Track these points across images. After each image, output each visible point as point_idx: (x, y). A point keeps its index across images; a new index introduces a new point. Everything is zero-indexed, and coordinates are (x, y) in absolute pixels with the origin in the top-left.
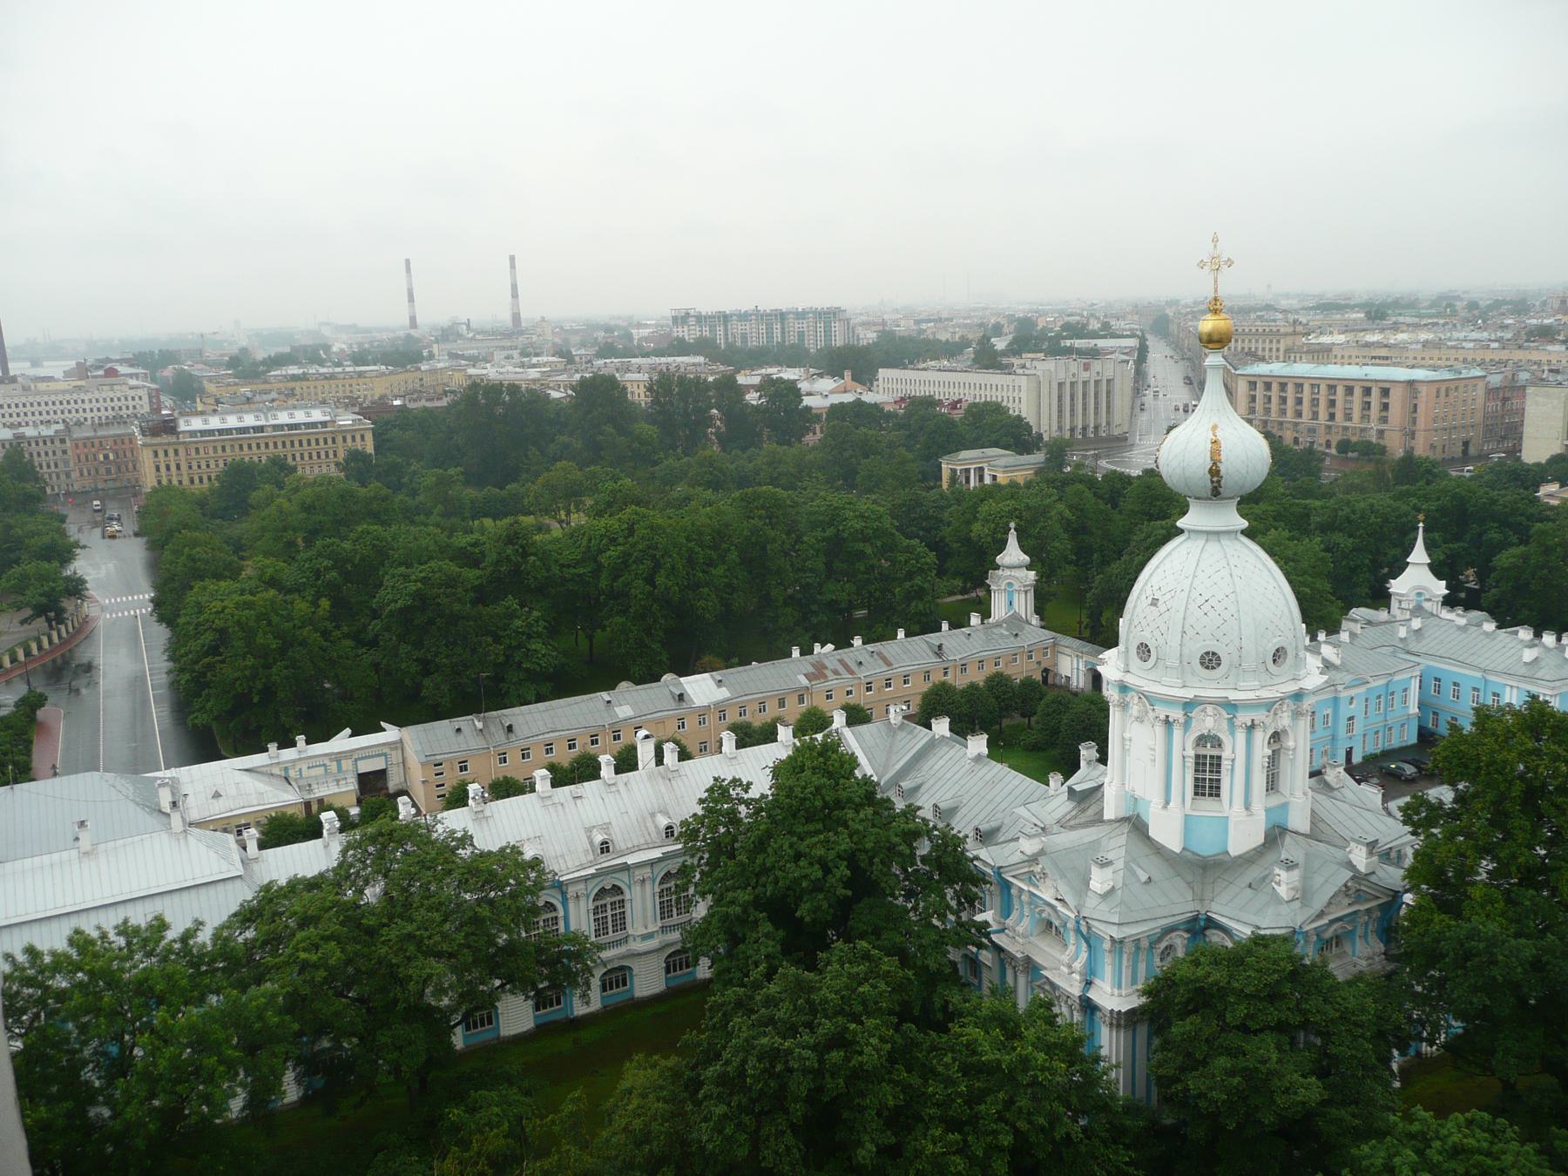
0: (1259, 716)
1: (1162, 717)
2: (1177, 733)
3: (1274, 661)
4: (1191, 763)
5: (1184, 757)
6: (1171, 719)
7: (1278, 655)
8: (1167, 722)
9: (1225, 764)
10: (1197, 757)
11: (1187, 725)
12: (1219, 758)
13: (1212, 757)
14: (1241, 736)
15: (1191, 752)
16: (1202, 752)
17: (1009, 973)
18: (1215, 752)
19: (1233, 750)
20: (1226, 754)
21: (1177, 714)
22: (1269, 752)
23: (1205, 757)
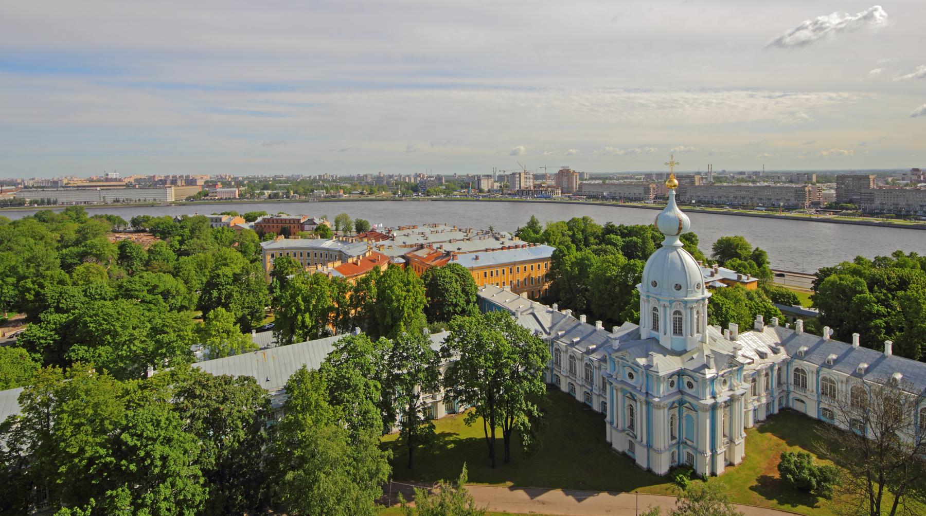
0: (695, 305)
2: (668, 309)
4: (672, 319)
8: (665, 307)
9: (684, 320)
11: (671, 307)
12: (681, 318)
14: (689, 311)
15: (672, 316)
17: (615, 391)
18: (680, 316)
19: (685, 314)
20: (684, 318)
21: (667, 304)
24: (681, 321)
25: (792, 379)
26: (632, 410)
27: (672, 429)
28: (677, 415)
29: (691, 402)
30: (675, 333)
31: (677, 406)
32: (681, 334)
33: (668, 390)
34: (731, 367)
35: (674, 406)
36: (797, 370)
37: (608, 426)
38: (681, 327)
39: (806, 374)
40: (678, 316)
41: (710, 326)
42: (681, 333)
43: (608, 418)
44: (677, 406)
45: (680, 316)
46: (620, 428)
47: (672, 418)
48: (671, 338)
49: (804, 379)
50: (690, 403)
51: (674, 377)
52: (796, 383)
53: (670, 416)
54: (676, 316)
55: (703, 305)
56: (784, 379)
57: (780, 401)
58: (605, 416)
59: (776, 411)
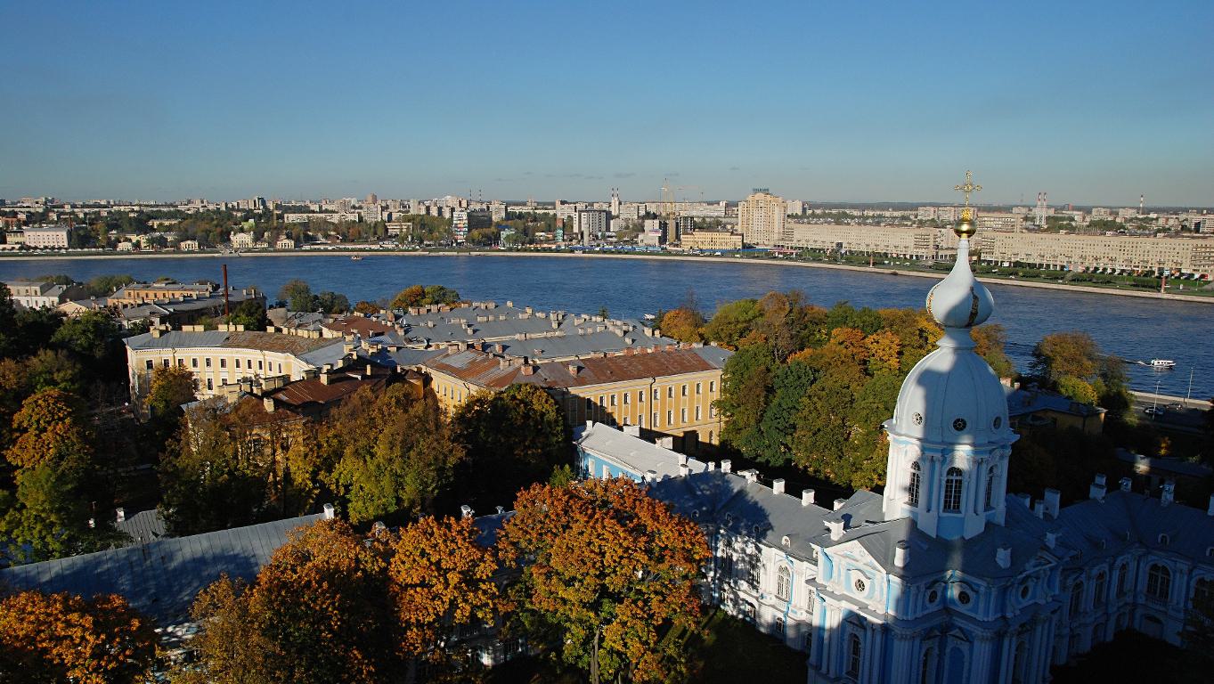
1: (930, 458)
2: (937, 465)
3: (995, 425)
4: (944, 483)
5: (940, 480)
6: (934, 458)
7: (997, 422)
9: (965, 484)
10: (948, 481)
12: (961, 481)
13: (956, 481)
15: (945, 478)
16: (951, 478)
18: (959, 478)
22: (988, 479)
23: (952, 481)
24: (960, 487)
25: (1142, 586)
26: (856, 644)
27: (924, 672)
28: (936, 651)
29: (962, 626)
30: (947, 507)
31: (938, 634)
32: (957, 508)
33: (924, 607)
34: (1040, 564)
35: (932, 635)
36: (1155, 567)
37: (811, 672)
38: (959, 497)
39: (1169, 575)
40: (954, 478)
41: (1012, 495)
42: (958, 507)
43: (813, 659)
44: (938, 634)
45: (959, 478)
46: (832, 675)
47: (926, 655)
48: (939, 517)
49: (1166, 583)
50: (960, 628)
51: (937, 585)
52: (1151, 589)
53: (923, 651)
54: (951, 478)
55: (1002, 457)
56: (1128, 586)
57: (1118, 620)
58: (809, 656)
59: (1110, 638)
